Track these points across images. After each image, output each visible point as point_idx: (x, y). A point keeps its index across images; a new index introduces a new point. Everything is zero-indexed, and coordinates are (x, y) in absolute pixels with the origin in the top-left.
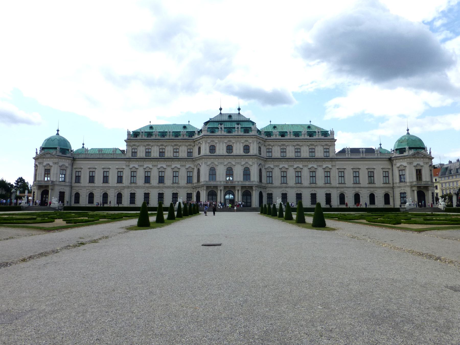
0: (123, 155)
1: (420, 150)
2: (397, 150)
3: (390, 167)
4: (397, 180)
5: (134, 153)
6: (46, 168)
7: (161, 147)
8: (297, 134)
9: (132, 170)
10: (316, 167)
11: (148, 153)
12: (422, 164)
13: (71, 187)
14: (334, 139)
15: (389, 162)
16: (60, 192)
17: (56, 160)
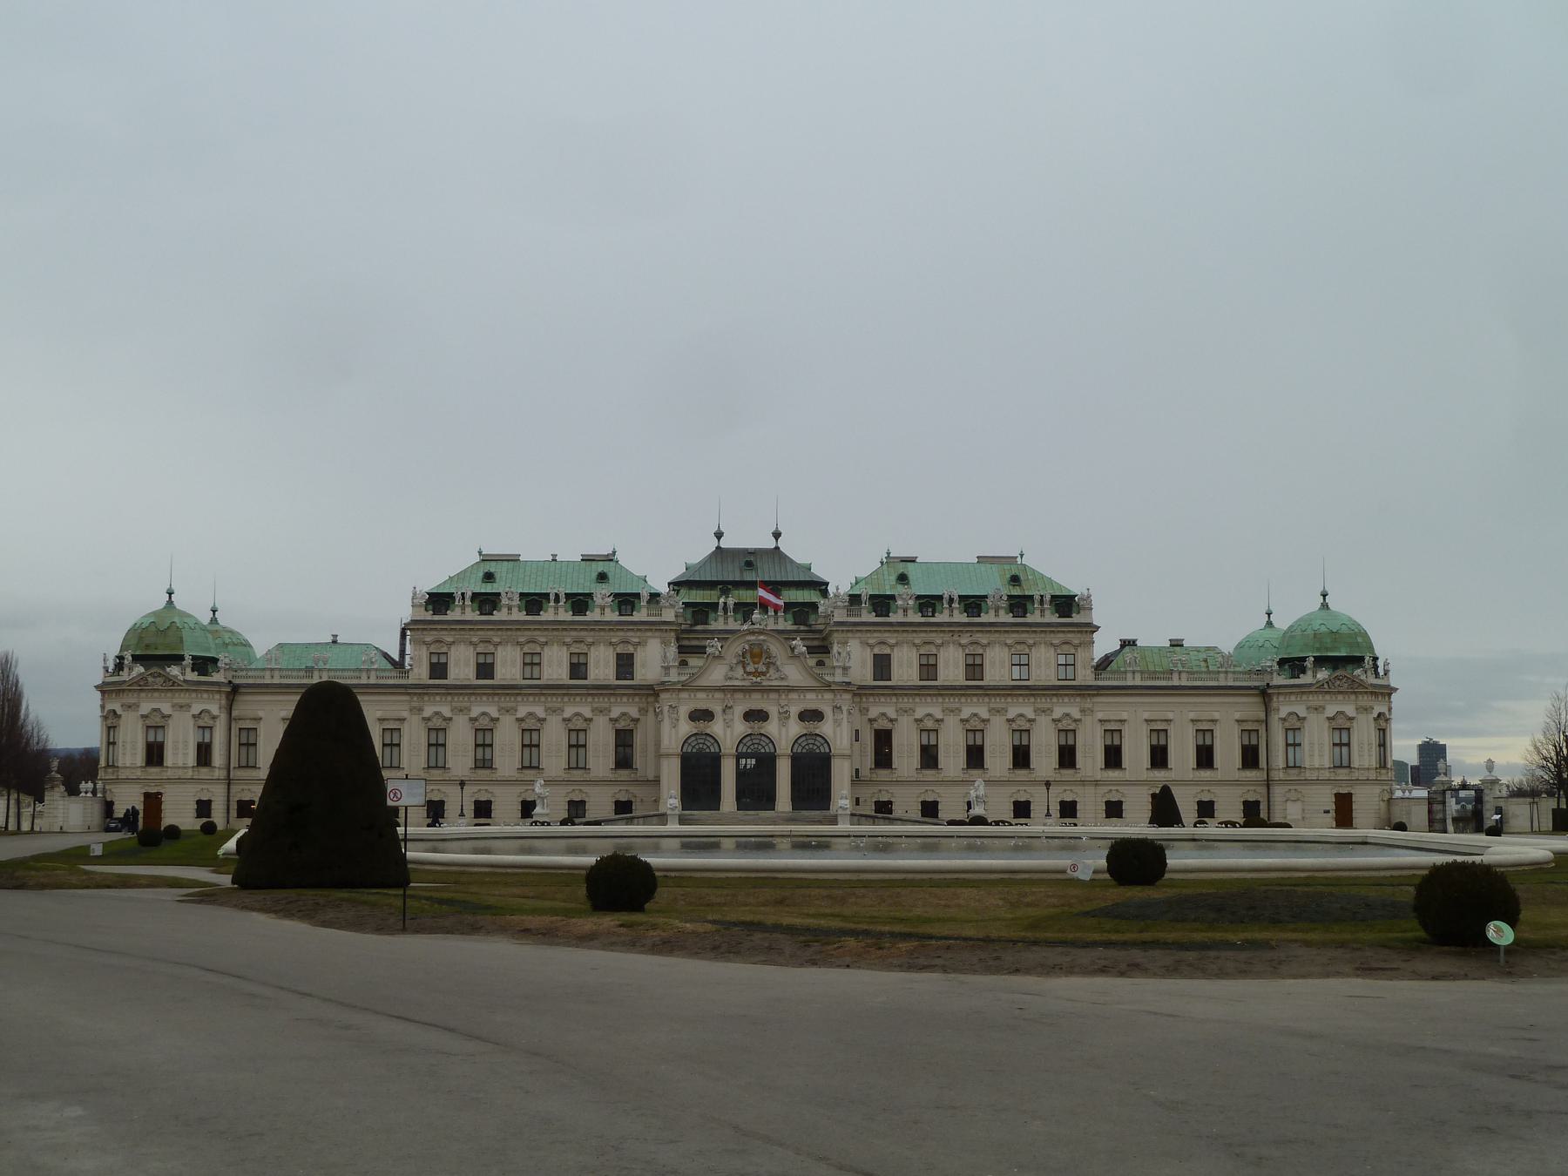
0: (394, 674)
1: (1349, 667)
2: (1282, 662)
3: (1262, 716)
5: (439, 670)
6: (149, 722)
7: (526, 649)
8: (973, 604)
9: (431, 725)
10: (1031, 715)
11: (485, 670)
12: (1350, 710)
13: (229, 781)
14: (1089, 625)
15: (1258, 699)
16: (199, 802)
17: (182, 699)
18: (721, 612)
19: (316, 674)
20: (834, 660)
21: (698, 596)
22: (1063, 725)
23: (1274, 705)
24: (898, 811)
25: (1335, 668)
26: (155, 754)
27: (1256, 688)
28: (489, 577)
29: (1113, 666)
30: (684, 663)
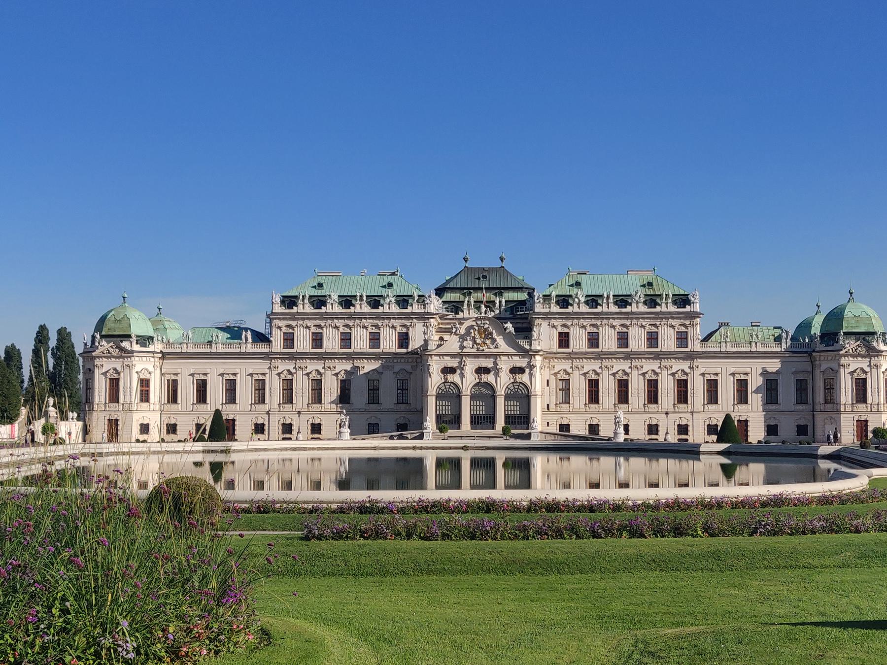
2: (823, 336)
4: (820, 398)
8: (622, 301)
16: (141, 425)
18: (465, 307)
19: (214, 346)
20: (535, 334)
21: (449, 296)
22: (679, 376)
23: (817, 363)
24: (574, 431)
25: (857, 340)
26: (114, 397)
27: (806, 352)
28: (320, 285)
29: (713, 339)
30: (441, 339)
